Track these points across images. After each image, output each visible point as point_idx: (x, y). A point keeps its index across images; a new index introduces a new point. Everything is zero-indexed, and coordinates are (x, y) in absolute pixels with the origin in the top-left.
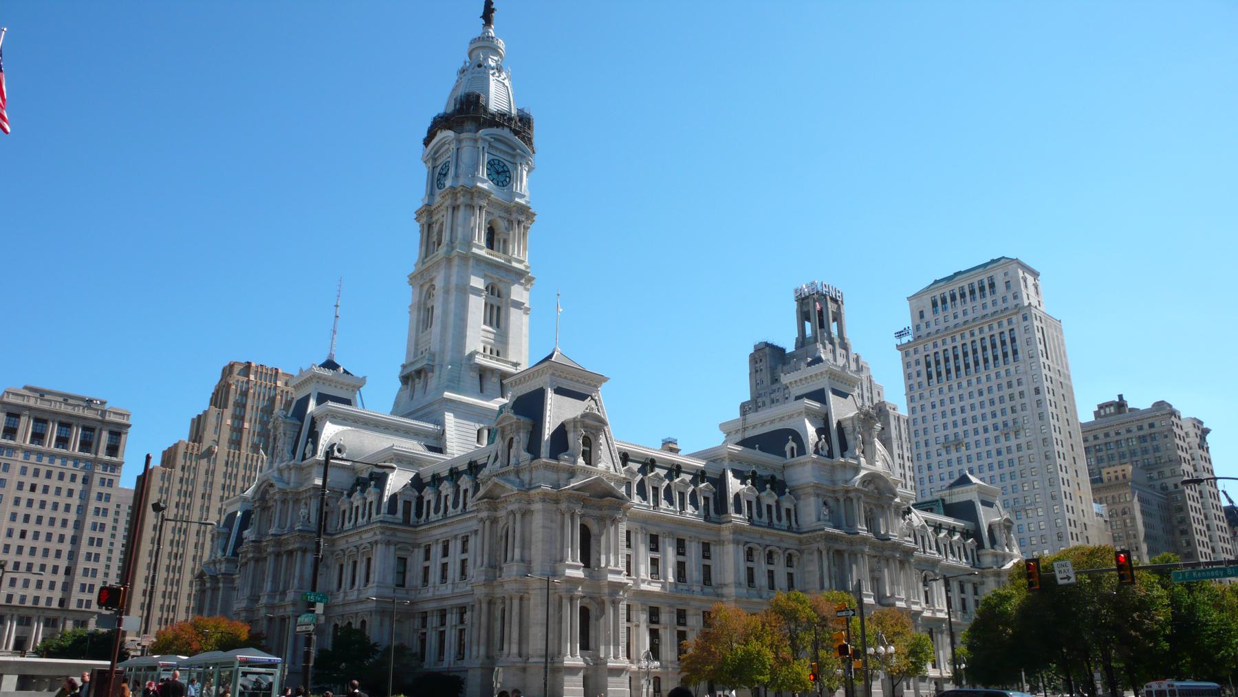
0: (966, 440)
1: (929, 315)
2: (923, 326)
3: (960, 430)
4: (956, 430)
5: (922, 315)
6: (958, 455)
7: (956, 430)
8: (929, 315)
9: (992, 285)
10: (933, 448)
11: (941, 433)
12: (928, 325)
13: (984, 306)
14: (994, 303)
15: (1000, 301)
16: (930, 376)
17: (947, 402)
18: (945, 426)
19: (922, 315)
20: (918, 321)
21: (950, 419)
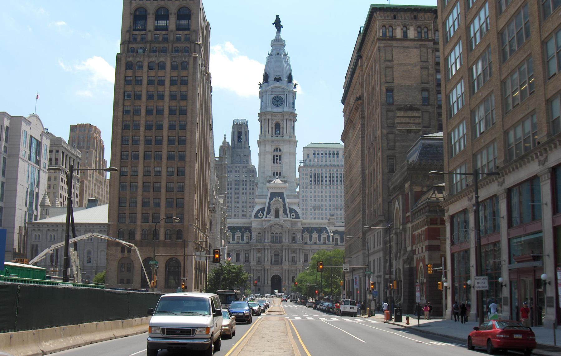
0: (322, 207)
1: (311, 157)
2: (308, 160)
3: (320, 203)
4: (319, 203)
5: (308, 156)
6: (318, 212)
7: (319, 203)
8: (311, 157)
9: (338, 154)
10: (309, 208)
11: (313, 203)
12: (310, 161)
13: (334, 161)
14: (338, 161)
15: (340, 161)
16: (311, 181)
17: (317, 192)
18: (315, 201)
19: (308, 156)
20: (306, 158)
21: (317, 198)
